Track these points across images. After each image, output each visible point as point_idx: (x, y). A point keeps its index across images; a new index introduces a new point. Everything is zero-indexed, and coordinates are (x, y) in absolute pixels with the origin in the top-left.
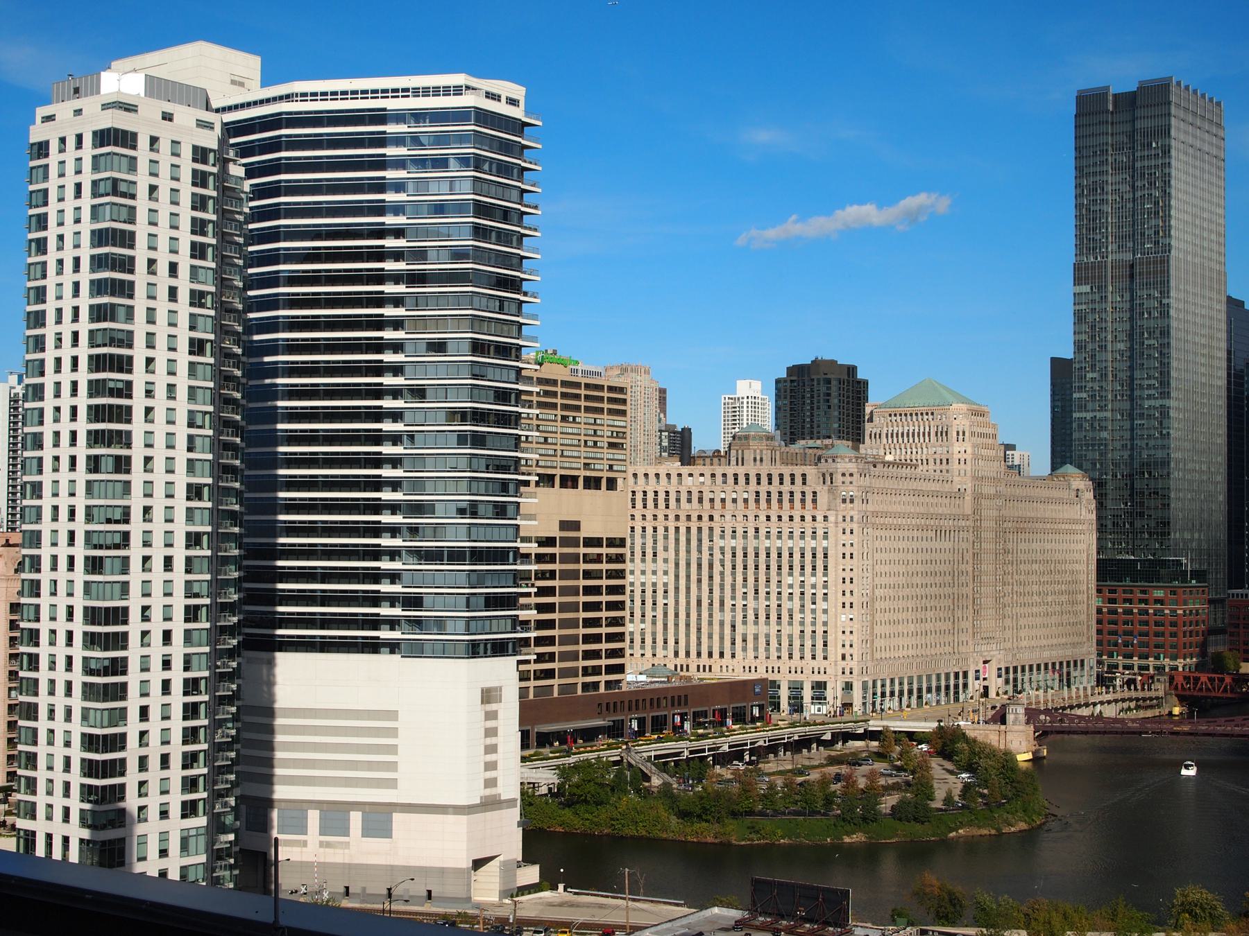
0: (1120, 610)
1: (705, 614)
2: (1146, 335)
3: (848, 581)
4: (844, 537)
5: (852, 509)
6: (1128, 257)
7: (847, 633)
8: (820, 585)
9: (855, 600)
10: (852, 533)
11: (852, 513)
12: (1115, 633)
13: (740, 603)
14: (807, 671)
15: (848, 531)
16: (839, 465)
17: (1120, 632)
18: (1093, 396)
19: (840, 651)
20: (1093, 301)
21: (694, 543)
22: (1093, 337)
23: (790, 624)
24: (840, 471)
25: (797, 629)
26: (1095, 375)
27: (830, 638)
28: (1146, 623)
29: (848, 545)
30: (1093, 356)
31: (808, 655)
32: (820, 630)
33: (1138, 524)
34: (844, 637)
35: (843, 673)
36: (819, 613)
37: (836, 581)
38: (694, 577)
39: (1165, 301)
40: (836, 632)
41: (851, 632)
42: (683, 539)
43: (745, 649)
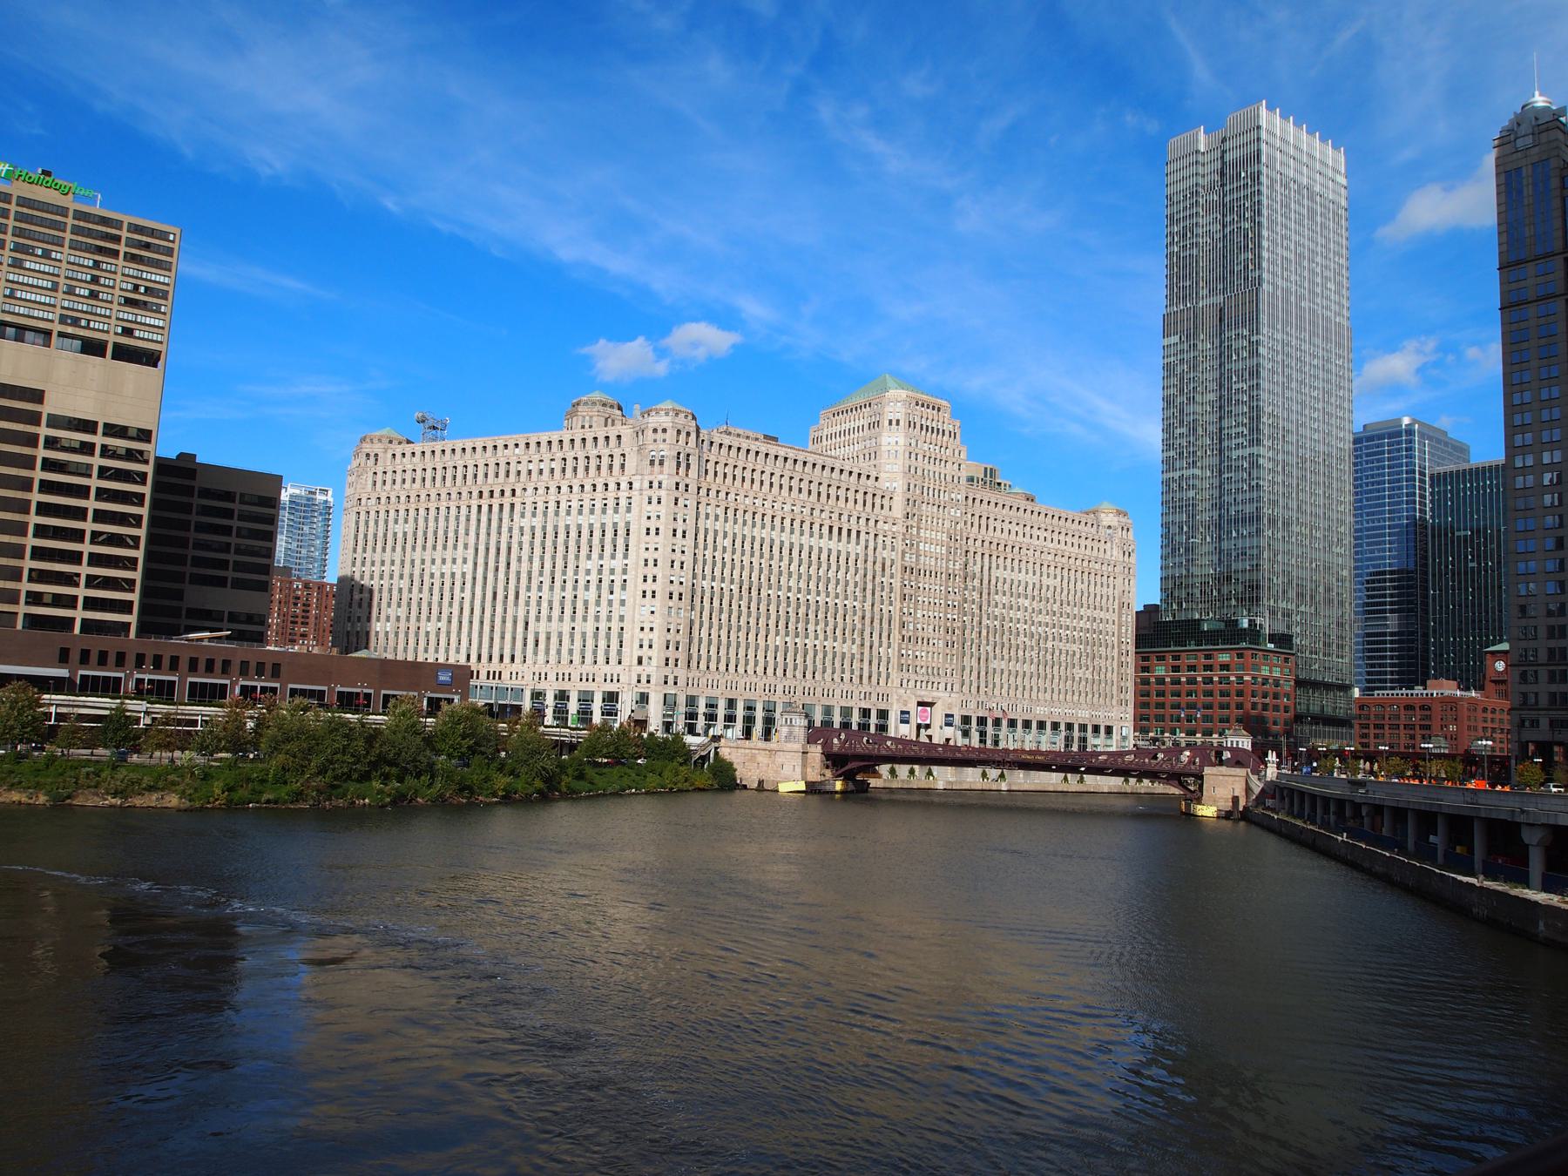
0: (1183, 679)
1: (499, 609)
2: (1234, 380)
3: (651, 563)
4: (649, 508)
5: (661, 473)
6: (1219, 299)
7: (647, 630)
8: (619, 570)
9: (657, 587)
10: (659, 502)
11: (661, 477)
12: (1178, 707)
13: (534, 594)
14: (575, 677)
15: (655, 500)
16: (651, 419)
17: (1183, 705)
18: (1181, 454)
19: (637, 653)
20: (1182, 351)
21: (494, 524)
22: (1181, 391)
23: (585, 619)
24: (651, 426)
25: (590, 627)
26: (1184, 430)
27: (626, 636)
28: (1209, 693)
29: (654, 518)
30: (1181, 411)
31: (601, 658)
32: (615, 625)
33: (1225, 590)
34: (641, 635)
35: (639, 681)
36: (616, 604)
37: (637, 564)
38: (491, 565)
39: (1254, 338)
40: (633, 628)
41: (652, 629)
42: (484, 518)
43: (536, 653)
